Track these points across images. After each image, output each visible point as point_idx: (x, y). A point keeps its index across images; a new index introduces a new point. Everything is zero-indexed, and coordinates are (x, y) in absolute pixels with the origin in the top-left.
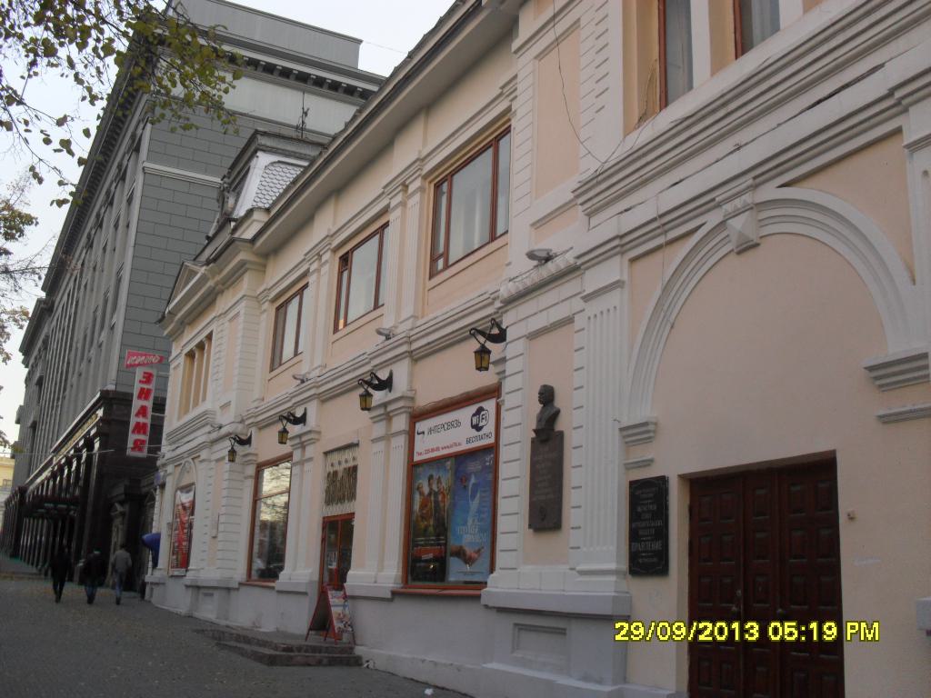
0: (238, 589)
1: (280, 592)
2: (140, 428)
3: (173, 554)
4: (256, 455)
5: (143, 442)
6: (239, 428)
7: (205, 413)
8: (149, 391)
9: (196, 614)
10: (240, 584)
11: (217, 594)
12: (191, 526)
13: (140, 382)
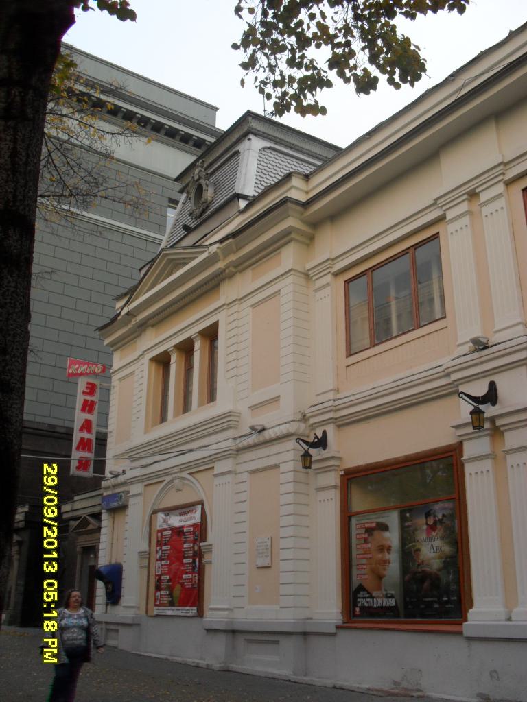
0: (334, 634)
1: (470, 639)
2: (84, 444)
3: (158, 588)
4: (340, 458)
5: (88, 462)
6: (302, 428)
7: (227, 415)
8: (93, 403)
9: (235, 667)
10: (338, 627)
11: (288, 645)
12: (199, 554)
13: (84, 393)
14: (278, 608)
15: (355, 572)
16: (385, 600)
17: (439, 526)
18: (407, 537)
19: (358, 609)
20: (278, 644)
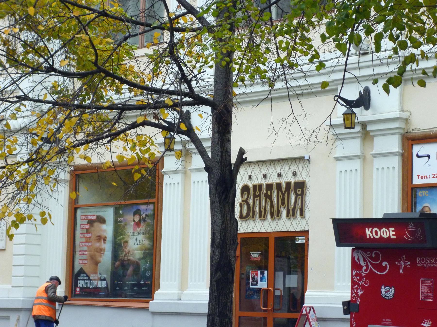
14: (11, 288)
15: (78, 256)
16: (99, 282)
17: (142, 224)
18: (119, 229)
19: (78, 289)
20: (9, 319)
